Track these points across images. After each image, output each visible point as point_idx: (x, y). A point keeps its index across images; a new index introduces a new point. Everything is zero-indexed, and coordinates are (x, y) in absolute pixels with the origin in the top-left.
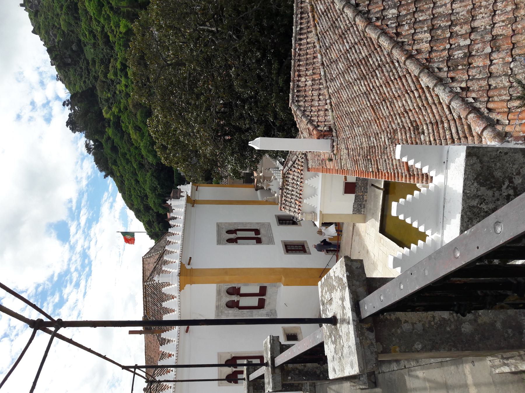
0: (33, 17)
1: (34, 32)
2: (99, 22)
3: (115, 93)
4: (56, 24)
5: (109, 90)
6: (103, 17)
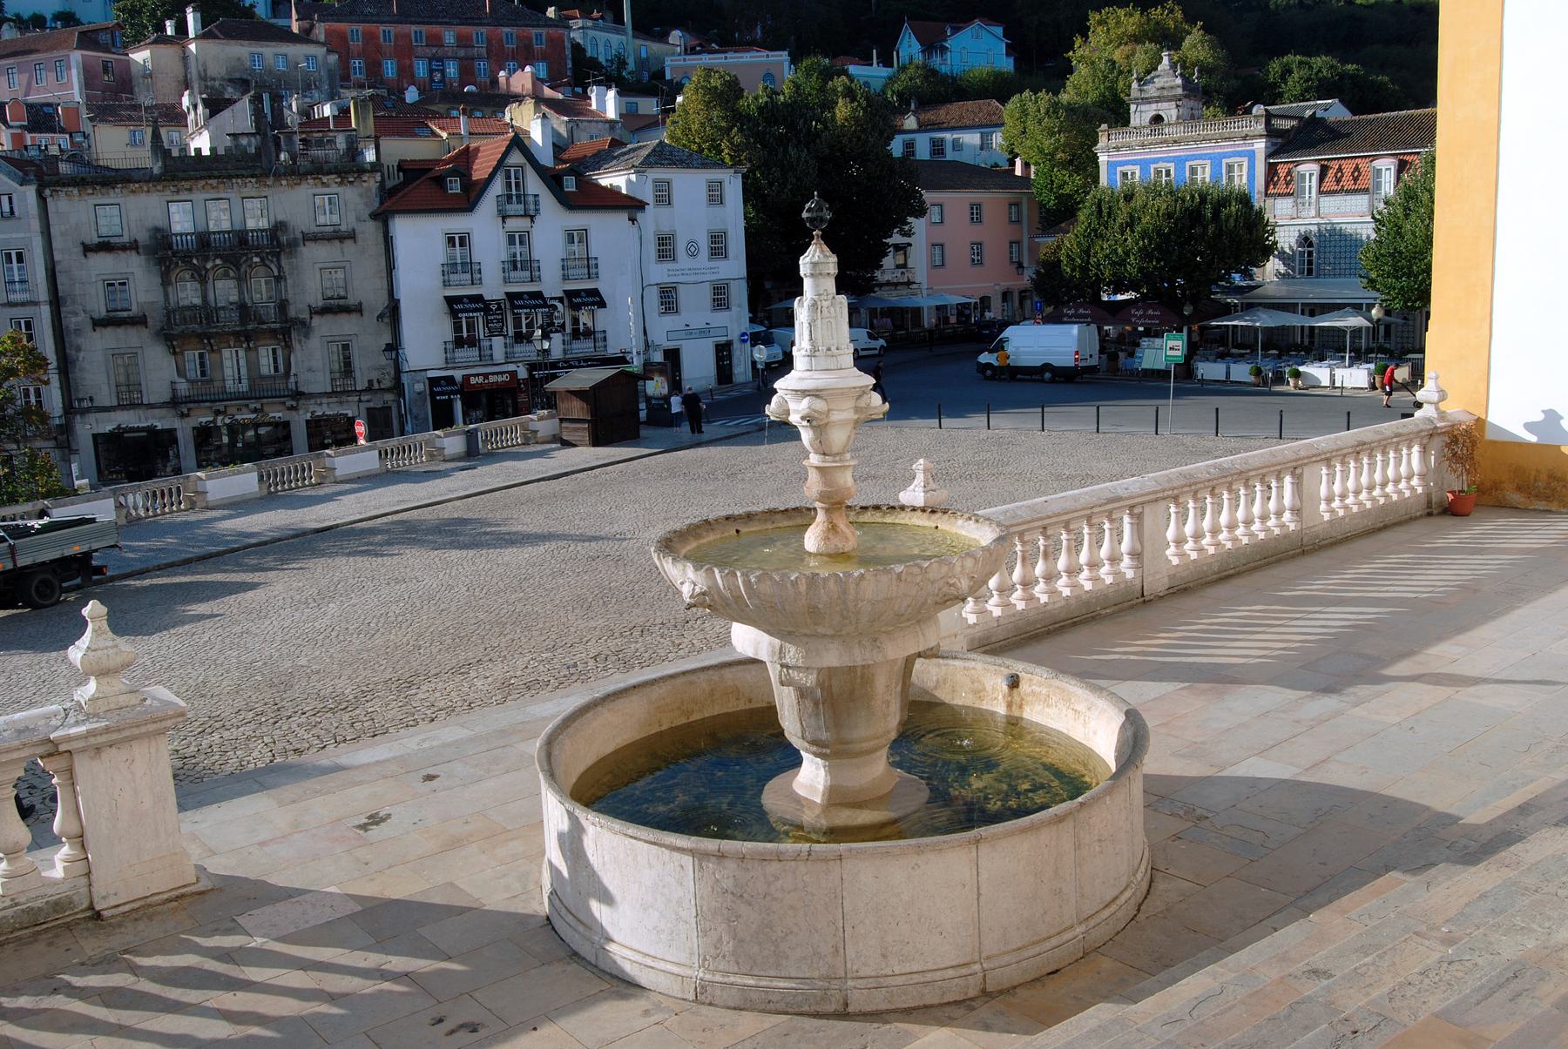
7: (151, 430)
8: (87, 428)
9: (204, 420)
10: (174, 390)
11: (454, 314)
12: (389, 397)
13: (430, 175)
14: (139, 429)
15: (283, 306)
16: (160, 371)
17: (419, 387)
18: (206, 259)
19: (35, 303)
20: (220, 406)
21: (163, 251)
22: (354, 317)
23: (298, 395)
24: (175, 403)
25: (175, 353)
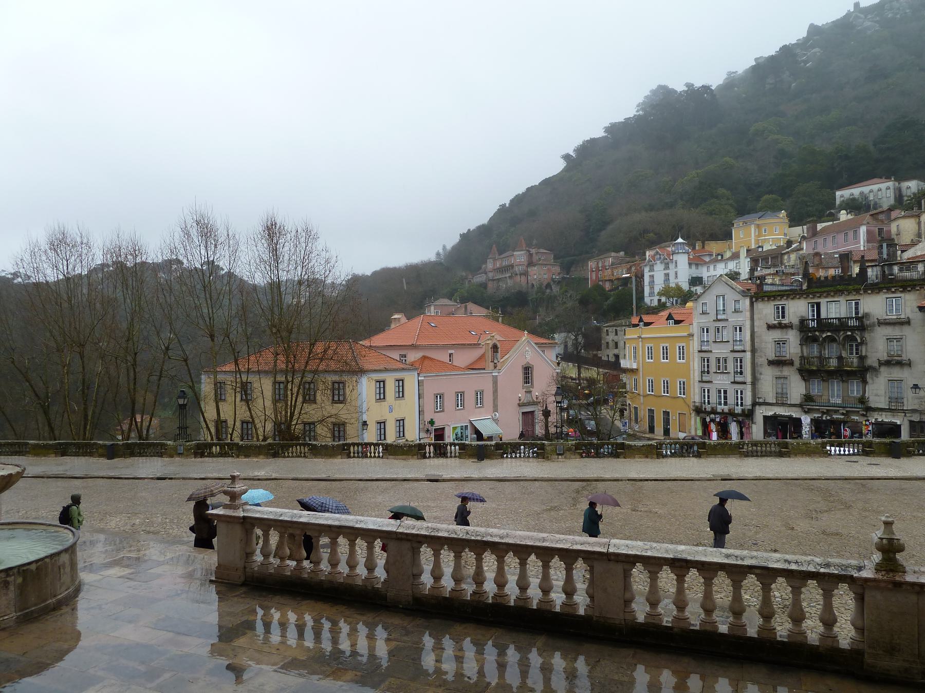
7: (790, 417)
8: (761, 413)
9: (816, 415)
14: (784, 416)
15: (862, 358)
16: (797, 389)
19: (744, 351)
23: (869, 409)
25: (804, 380)
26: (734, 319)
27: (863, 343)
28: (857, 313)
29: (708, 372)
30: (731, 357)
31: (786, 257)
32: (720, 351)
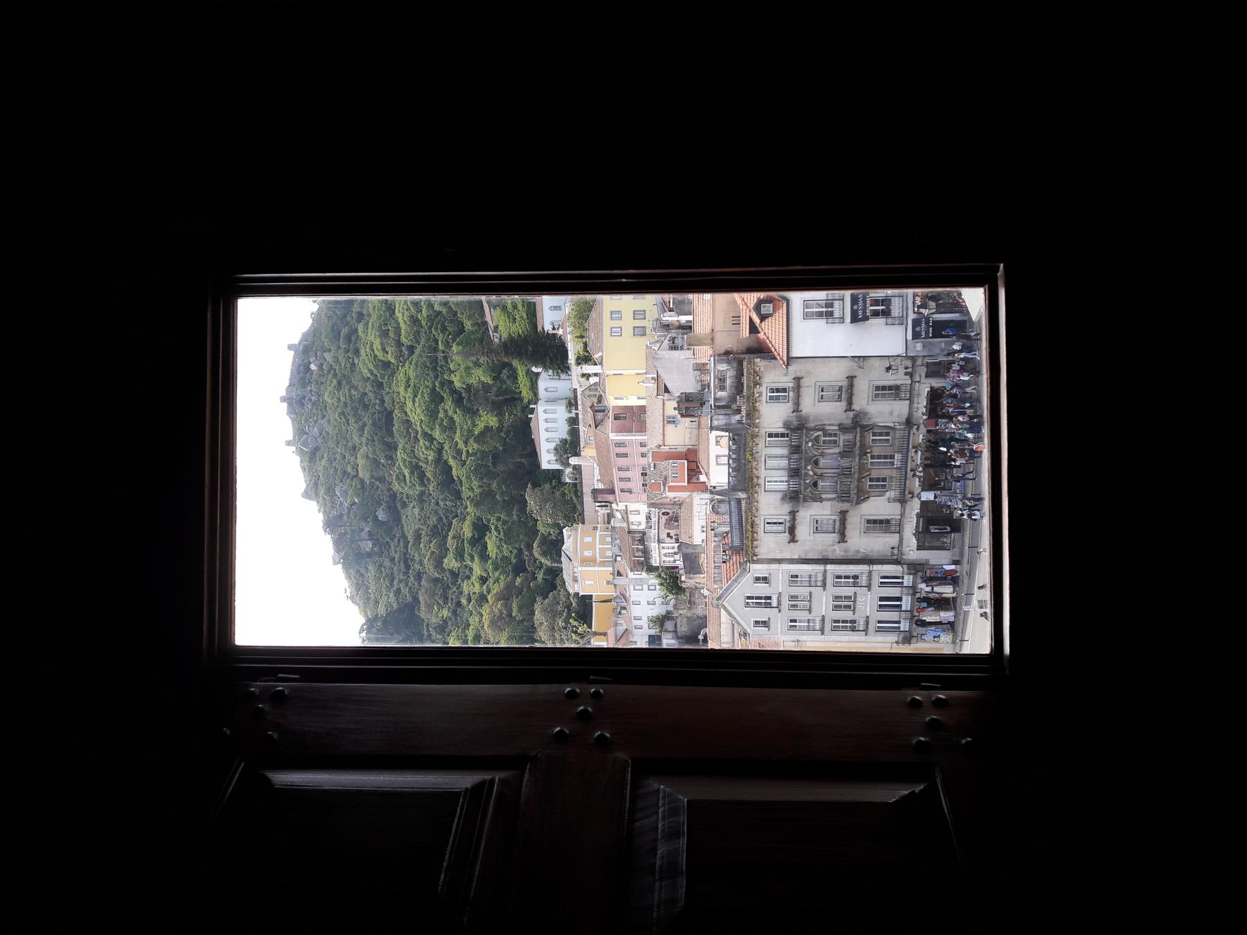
0: (306, 464)
1: (306, 495)
2: (431, 439)
3: (459, 604)
4: (349, 469)
5: (446, 599)
6: (441, 425)
7: (919, 516)
8: (912, 551)
10: (894, 501)
11: (866, 318)
12: (919, 362)
13: (757, 320)
14: (918, 523)
15: (843, 428)
16: (879, 506)
17: (919, 346)
18: (806, 474)
20: (910, 474)
21: (793, 497)
22: (856, 382)
23: (909, 422)
24: (902, 501)
26: (779, 586)
27: (823, 430)
28: (783, 435)
29: (853, 622)
30: (832, 590)
31: (633, 527)
32: (823, 603)
